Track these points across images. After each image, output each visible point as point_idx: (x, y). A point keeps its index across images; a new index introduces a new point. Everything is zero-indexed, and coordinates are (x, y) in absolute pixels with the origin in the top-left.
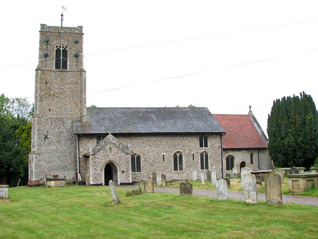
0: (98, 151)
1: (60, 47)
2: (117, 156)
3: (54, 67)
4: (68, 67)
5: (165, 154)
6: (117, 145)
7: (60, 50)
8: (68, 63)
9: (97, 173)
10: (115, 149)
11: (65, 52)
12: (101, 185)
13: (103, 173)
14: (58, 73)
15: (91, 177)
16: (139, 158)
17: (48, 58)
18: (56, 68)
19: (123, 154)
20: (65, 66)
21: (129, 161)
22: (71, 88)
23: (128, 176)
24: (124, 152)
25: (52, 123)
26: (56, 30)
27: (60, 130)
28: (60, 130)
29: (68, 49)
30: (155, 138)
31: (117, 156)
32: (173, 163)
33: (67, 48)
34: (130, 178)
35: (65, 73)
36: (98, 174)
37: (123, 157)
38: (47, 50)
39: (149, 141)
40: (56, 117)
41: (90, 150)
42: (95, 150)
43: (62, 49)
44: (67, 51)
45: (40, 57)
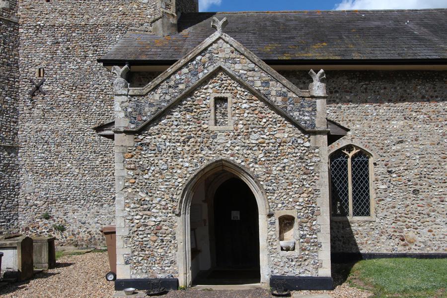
0: (156, 119)
2: (254, 138)
9: (151, 222)
12: (172, 284)
13: (181, 228)
15: (119, 243)
16: (362, 159)
19: (287, 132)
21: (317, 164)
23: (310, 243)
31: (254, 138)
34: (325, 255)
36: (158, 227)
37: (286, 149)
41: (117, 107)
42: (138, 109)
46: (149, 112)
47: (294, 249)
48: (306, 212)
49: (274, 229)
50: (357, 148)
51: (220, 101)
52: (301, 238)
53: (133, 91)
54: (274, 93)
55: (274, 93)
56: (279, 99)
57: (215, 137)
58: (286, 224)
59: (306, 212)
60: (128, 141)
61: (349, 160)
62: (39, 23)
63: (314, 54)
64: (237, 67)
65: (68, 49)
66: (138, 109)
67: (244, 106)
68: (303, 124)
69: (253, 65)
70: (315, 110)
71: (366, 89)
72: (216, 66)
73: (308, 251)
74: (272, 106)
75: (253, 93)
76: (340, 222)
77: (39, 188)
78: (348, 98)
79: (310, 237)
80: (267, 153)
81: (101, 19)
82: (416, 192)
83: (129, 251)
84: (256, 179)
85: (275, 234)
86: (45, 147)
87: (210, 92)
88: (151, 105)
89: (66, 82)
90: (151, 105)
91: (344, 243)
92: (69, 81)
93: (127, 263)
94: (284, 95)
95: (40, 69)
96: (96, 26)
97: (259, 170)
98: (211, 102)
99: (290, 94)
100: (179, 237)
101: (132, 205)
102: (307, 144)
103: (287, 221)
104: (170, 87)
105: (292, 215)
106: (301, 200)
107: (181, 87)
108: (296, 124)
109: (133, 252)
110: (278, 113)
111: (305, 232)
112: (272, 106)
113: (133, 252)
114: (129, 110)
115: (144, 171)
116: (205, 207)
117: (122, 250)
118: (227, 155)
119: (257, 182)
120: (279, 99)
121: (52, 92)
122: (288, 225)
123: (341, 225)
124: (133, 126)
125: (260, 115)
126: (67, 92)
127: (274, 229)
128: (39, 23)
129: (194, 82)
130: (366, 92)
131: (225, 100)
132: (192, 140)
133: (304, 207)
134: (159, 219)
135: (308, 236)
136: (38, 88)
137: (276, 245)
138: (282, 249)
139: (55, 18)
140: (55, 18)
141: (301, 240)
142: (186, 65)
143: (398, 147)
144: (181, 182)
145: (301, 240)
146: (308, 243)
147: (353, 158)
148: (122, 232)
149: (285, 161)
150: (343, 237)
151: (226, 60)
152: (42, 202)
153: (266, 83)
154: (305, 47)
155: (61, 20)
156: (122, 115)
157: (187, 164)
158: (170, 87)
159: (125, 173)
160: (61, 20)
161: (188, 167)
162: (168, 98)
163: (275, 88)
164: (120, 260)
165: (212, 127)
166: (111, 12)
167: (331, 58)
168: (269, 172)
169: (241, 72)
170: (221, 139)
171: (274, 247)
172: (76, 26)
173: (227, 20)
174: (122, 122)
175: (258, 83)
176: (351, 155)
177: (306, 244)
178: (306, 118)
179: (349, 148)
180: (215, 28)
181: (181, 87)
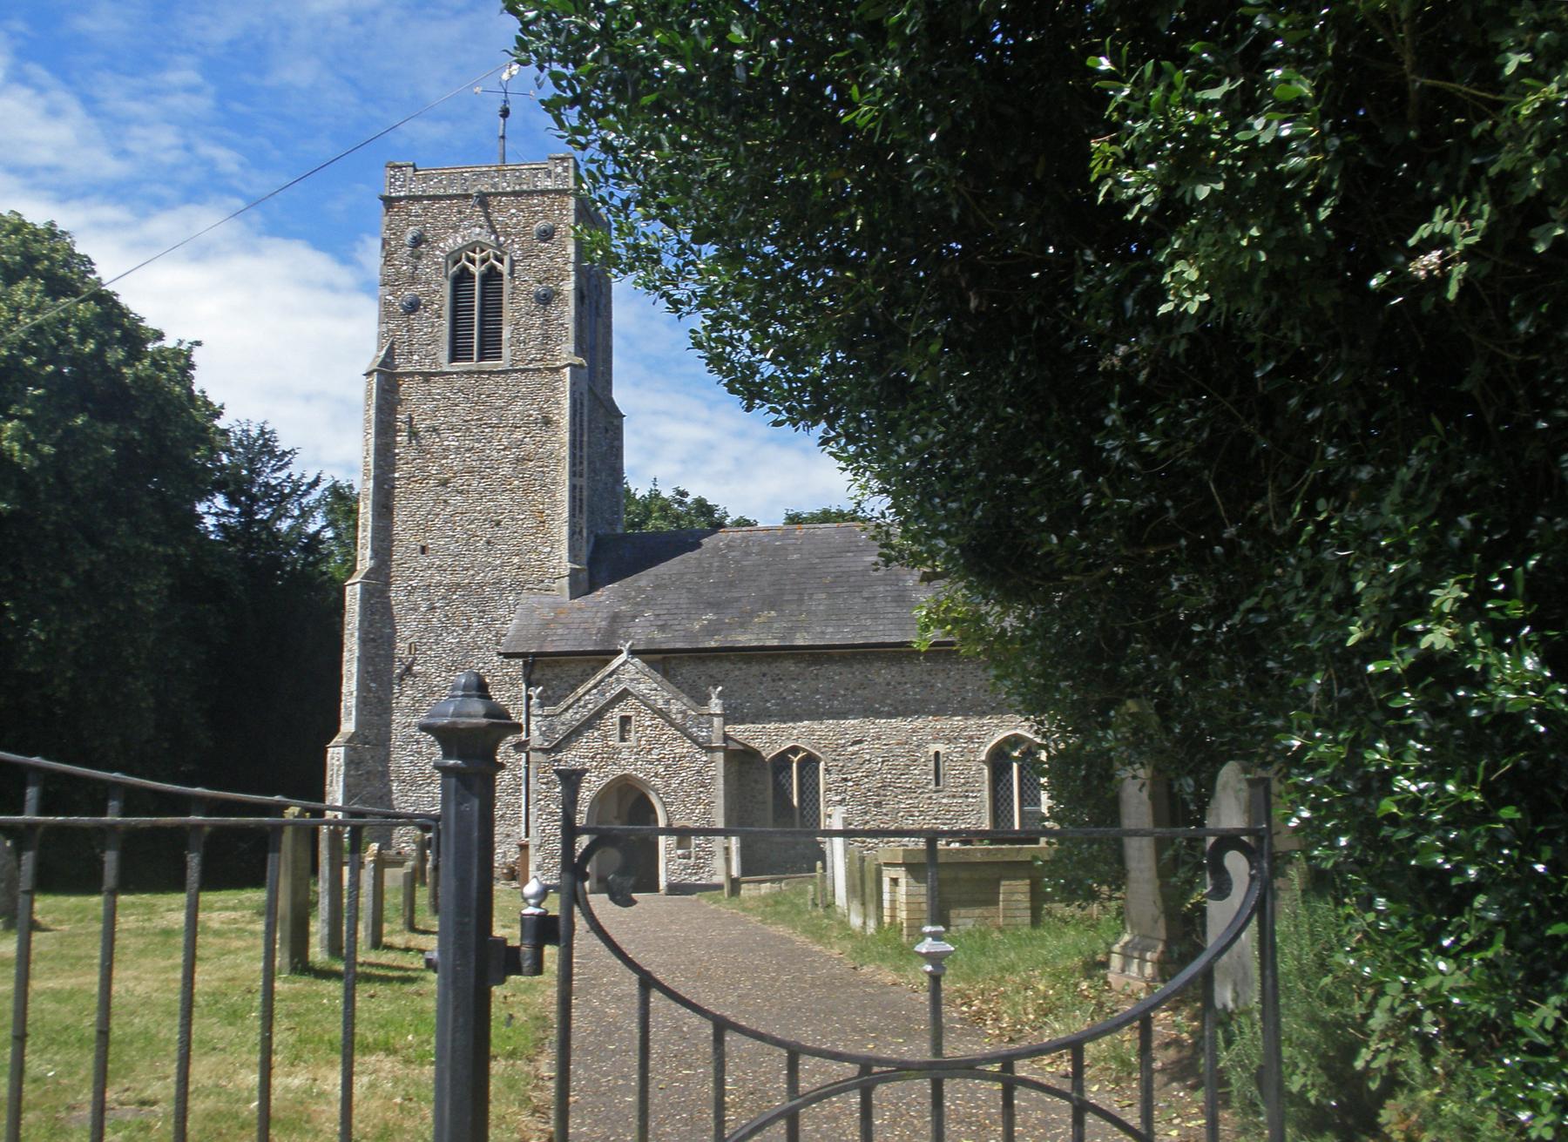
1: (472, 261)
3: (444, 354)
4: (506, 351)
5: (941, 747)
6: (660, 704)
7: (472, 276)
8: (506, 333)
10: (645, 721)
11: (492, 276)
14: (459, 382)
17: (420, 321)
18: (454, 357)
20: (490, 346)
22: (519, 444)
24: (690, 736)
25: (432, 608)
26: (451, 184)
27: (467, 638)
28: (467, 638)
29: (504, 268)
30: (895, 670)
32: (986, 794)
33: (501, 261)
35: (490, 384)
38: (413, 279)
39: (862, 686)
40: (448, 579)
42: (551, 728)
43: (476, 270)
44: (500, 275)
45: (386, 314)
46: (561, 732)
51: (625, 721)
53: (548, 710)
64: (642, 686)
66: (551, 728)
72: (623, 686)
75: (655, 712)
80: (667, 767)
82: (878, 804)
84: (656, 791)
94: (684, 712)
97: (658, 782)
98: (617, 720)
108: (695, 741)
118: (630, 770)
129: (602, 702)
131: (629, 718)
142: (595, 687)
143: (856, 748)
153: (667, 702)
163: (675, 707)
167: (768, 643)
168: (669, 785)
175: (660, 702)
179: (795, 750)
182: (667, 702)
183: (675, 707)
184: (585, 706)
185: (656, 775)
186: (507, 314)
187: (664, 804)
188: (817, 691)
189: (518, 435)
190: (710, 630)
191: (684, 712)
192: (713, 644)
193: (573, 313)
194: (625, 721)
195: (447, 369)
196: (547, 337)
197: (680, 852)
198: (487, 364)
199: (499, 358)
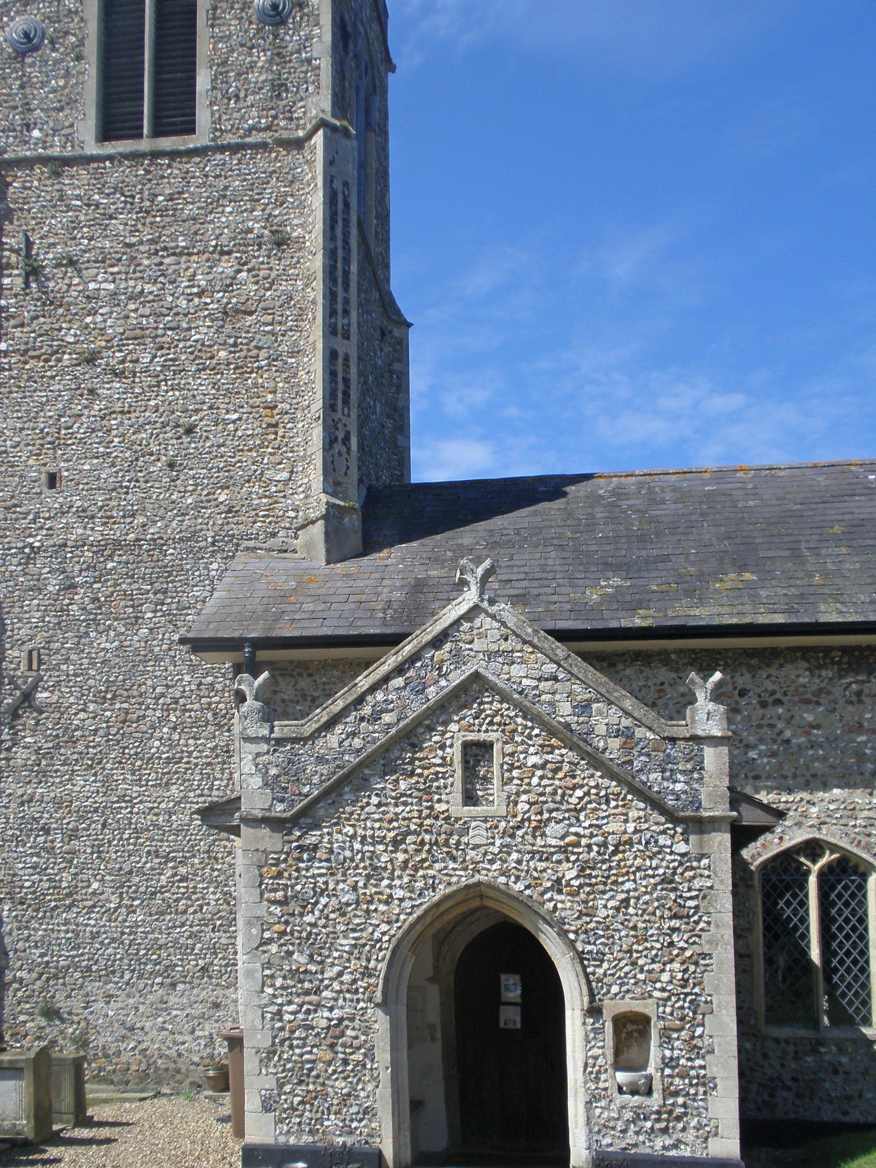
4: (203, 117)
8: (203, 81)
9: (320, 1020)
14: (115, 175)
15: (250, 1062)
18: (106, 134)
19: (629, 819)
20: (176, 114)
24: (642, 793)
42: (292, 771)
46: (315, 778)
47: (649, 1092)
48: (677, 1005)
49: (601, 1044)
50: (834, 848)
52: (667, 1065)
53: (282, 728)
54: (601, 729)
55: (601, 729)
56: (615, 743)
57: (465, 831)
58: (630, 1034)
59: (677, 1005)
60: (269, 840)
61: (813, 882)
62: (31, 540)
63: (714, 610)
64: (517, 671)
65: (95, 600)
66: (292, 771)
67: (533, 760)
68: (670, 802)
69: (550, 668)
70: (699, 767)
71: (859, 694)
72: (468, 670)
73: (684, 1096)
74: (596, 761)
75: (552, 732)
76: (787, 1042)
77: (27, 940)
78: (809, 718)
79: (689, 1064)
81: (174, 524)
83: (270, 1083)
85: (603, 1054)
86: (41, 839)
87: (456, 734)
88: (321, 760)
89: (91, 682)
90: (321, 760)
91: (799, 1095)
92: (96, 681)
93: (267, 1107)
94: (627, 735)
95: (30, 652)
96: (159, 544)
98: (455, 753)
99: (640, 733)
100: (383, 1056)
101: (279, 982)
102: (682, 848)
103: (635, 1027)
104: (362, 719)
105: (646, 1011)
106: (665, 977)
107: (387, 718)
109: (281, 1086)
110: (610, 774)
111: (676, 1053)
112: (596, 761)
113: (281, 1086)
114: (273, 771)
115: (306, 906)
116: (434, 993)
117: (257, 1082)
119: (563, 934)
120: (615, 743)
121: (57, 707)
122: (635, 1034)
123: (791, 1049)
124: (280, 807)
125: (570, 782)
126: (92, 707)
127: (601, 1044)
128: (31, 540)
129: (416, 708)
130: (860, 701)
131: (488, 746)
132: (410, 839)
133: (673, 994)
134: (337, 1013)
135: (682, 1061)
136: (27, 697)
137: (605, 1081)
138: (620, 1090)
139: (68, 527)
140: (68, 527)
141: (667, 1071)
142: (399, 670)
144: (385, 933)
145: (667, 1071)
146: (682, 1077)
147: (821, 875)
148: (256, 1040)
149: (629, 885)
150: (795, 1080)
151: (491, 655)
152: (34, 975)
153: (584, 708)
154: (693, 591)
155: (80, 531)
156: (257, 782)
157: (400, 893)
158: (362, 719)
159: (262, 910)
160: (80, 531)
161: (404, 902)
162: (357, 742)
163: (604, 720)
164: (252, 1103)
165: (459, 810)
166: (198, 506)
168: (590, 913)
169: (525, 682)
170: (478, 835)
171: (601, 1085)
172: (118, 544)
173: (493, 566)
174: (255, 797)
175: (565, 708)
176: (816, 868)
177: (677, 1081)
178: (679, 787)
179: (813, 848)
180: (464, 583)
181: (387, 718)
182: (584, 708)
183: (604, 720)
184: (375, 717)
185: (558, 885)
186: (204, 47)
187: (581, 957)
188: (860, 727)
189: (226, 266)
190: (618, 600)
191: (627, 735)
192: (638, 622)
193: (328, 38)
194: (476, 753)
195: (92, 149)
196: (279, 87)
197: (622, 1077)
198: (167, 143)
199: (192, 131)
